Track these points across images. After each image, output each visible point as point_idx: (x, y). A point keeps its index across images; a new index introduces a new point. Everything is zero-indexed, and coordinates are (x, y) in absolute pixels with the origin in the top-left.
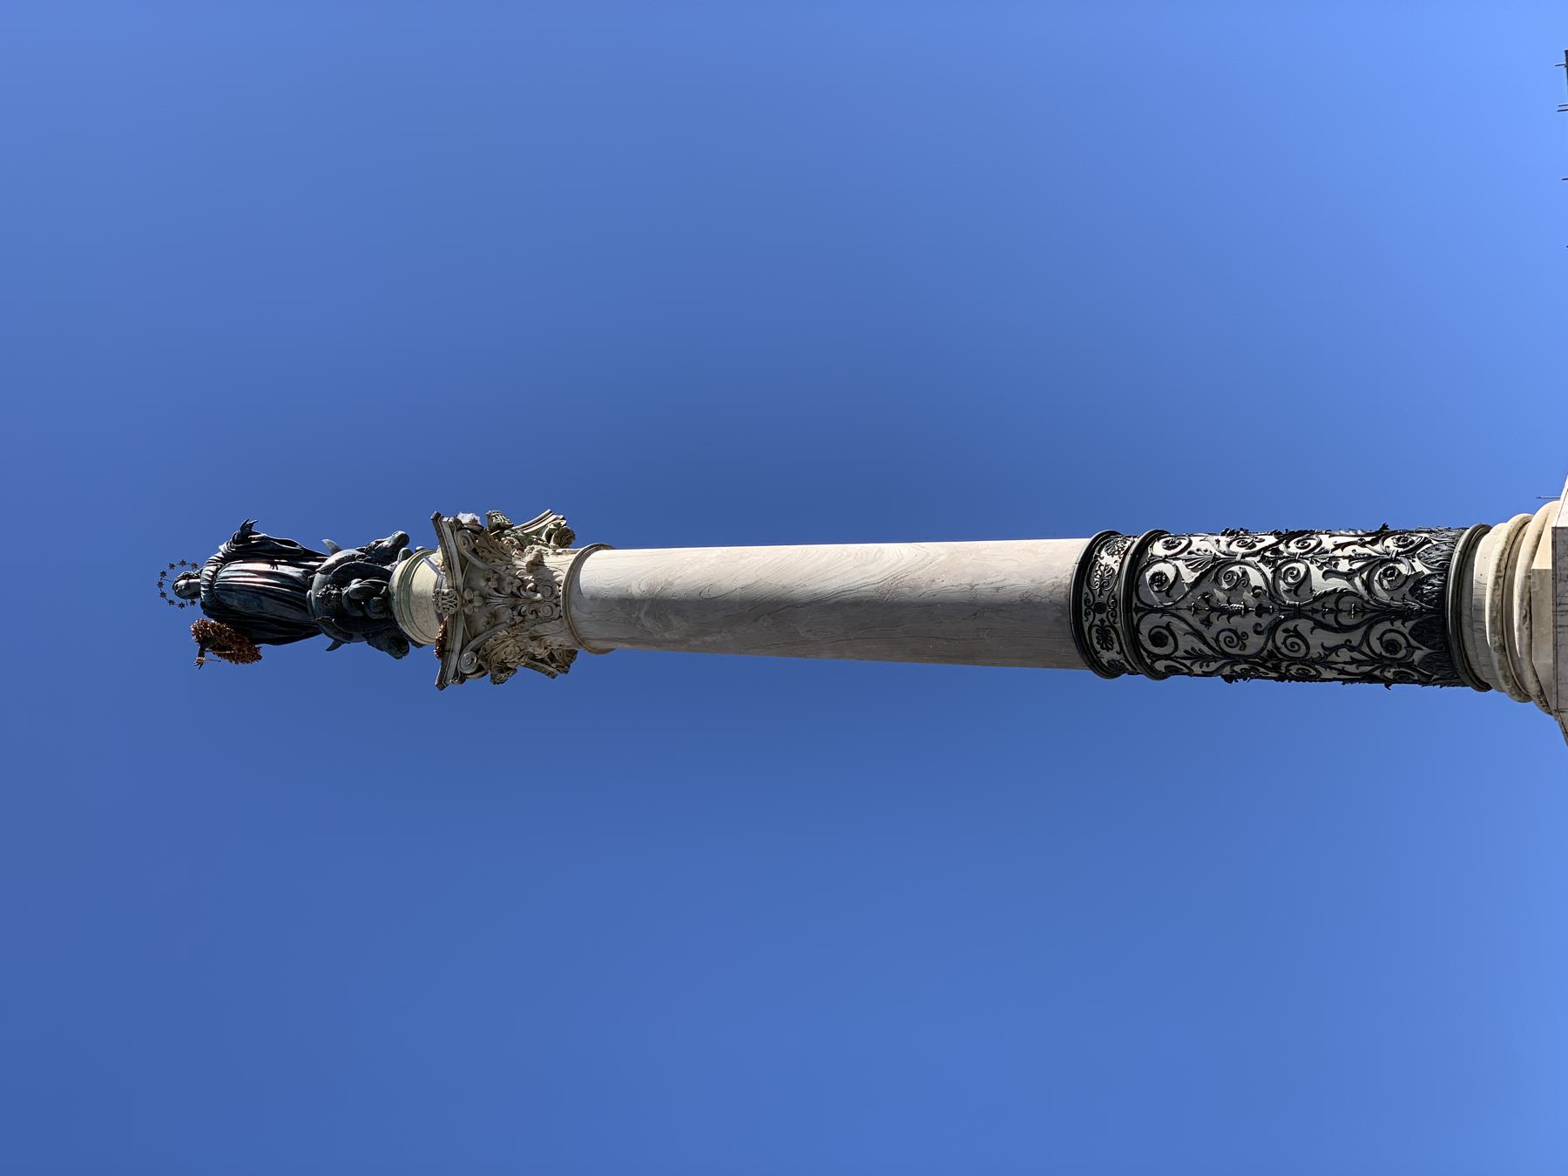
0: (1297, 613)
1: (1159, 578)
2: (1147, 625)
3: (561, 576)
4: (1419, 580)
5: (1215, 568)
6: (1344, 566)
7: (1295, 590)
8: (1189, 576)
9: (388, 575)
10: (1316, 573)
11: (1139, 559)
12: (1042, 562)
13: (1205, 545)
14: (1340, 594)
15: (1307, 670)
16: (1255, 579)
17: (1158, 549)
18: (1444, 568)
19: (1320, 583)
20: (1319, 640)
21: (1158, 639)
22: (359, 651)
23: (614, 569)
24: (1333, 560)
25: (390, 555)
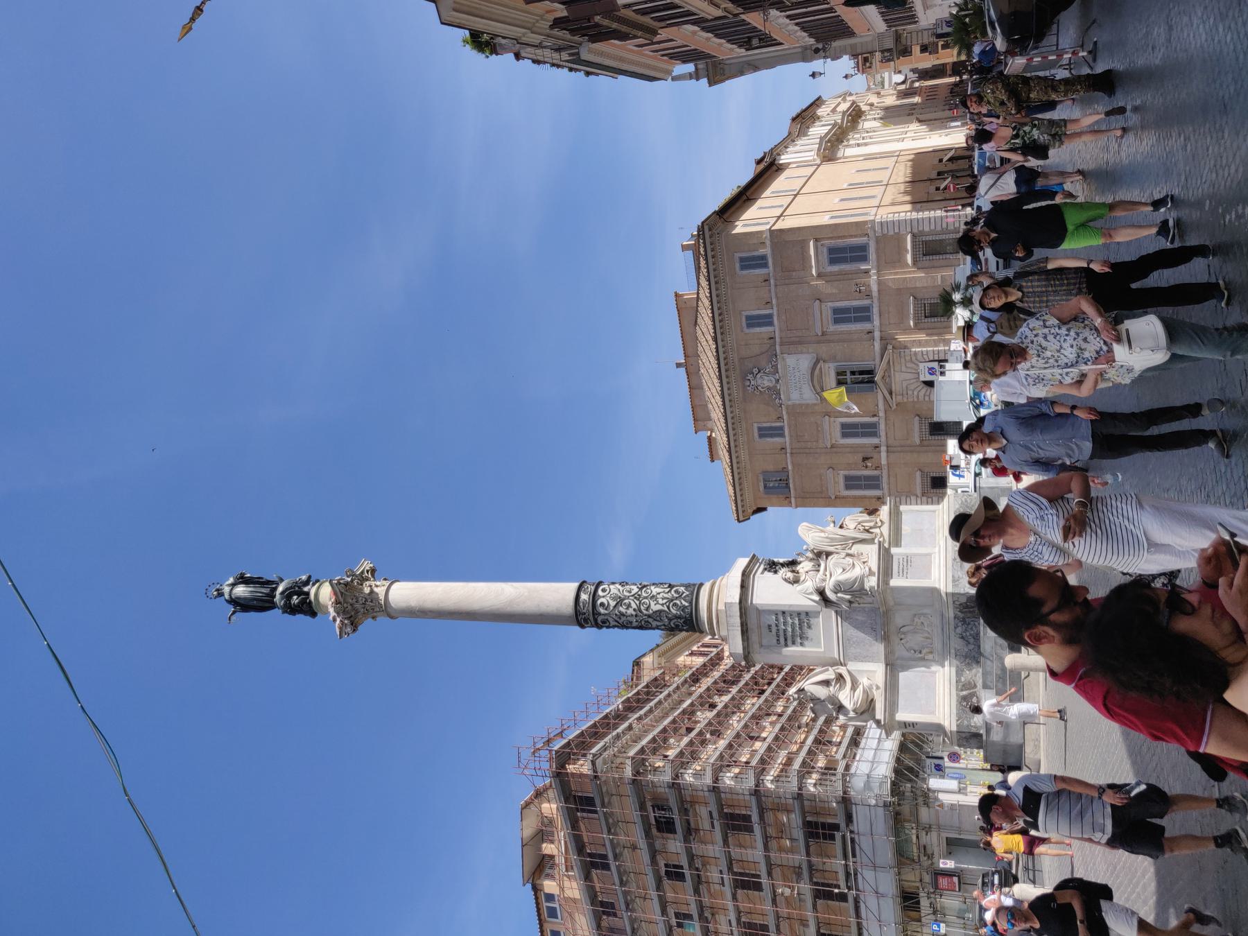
0: (649, 616)
1: (602, 604)
2: (600, 619)
3: (382, 597)
4: (685, 607)
5: (620, 601)
6: (661, 601)
7: (647, 609)
8: (613, 603)
9: (308, 594)
10: (652, 604)
11: (595, 596)
12: (558, 594)
13: (615, 589)
14: (660, 611)
16: (634, 606)
17: (600, 593)
18: (691, 603)
19: (655, 607)
20: (654, 624)
21: (604, 622)
22: (300, 617)
23: (403, 593)
24: (658, 599)
25: (307, 583)
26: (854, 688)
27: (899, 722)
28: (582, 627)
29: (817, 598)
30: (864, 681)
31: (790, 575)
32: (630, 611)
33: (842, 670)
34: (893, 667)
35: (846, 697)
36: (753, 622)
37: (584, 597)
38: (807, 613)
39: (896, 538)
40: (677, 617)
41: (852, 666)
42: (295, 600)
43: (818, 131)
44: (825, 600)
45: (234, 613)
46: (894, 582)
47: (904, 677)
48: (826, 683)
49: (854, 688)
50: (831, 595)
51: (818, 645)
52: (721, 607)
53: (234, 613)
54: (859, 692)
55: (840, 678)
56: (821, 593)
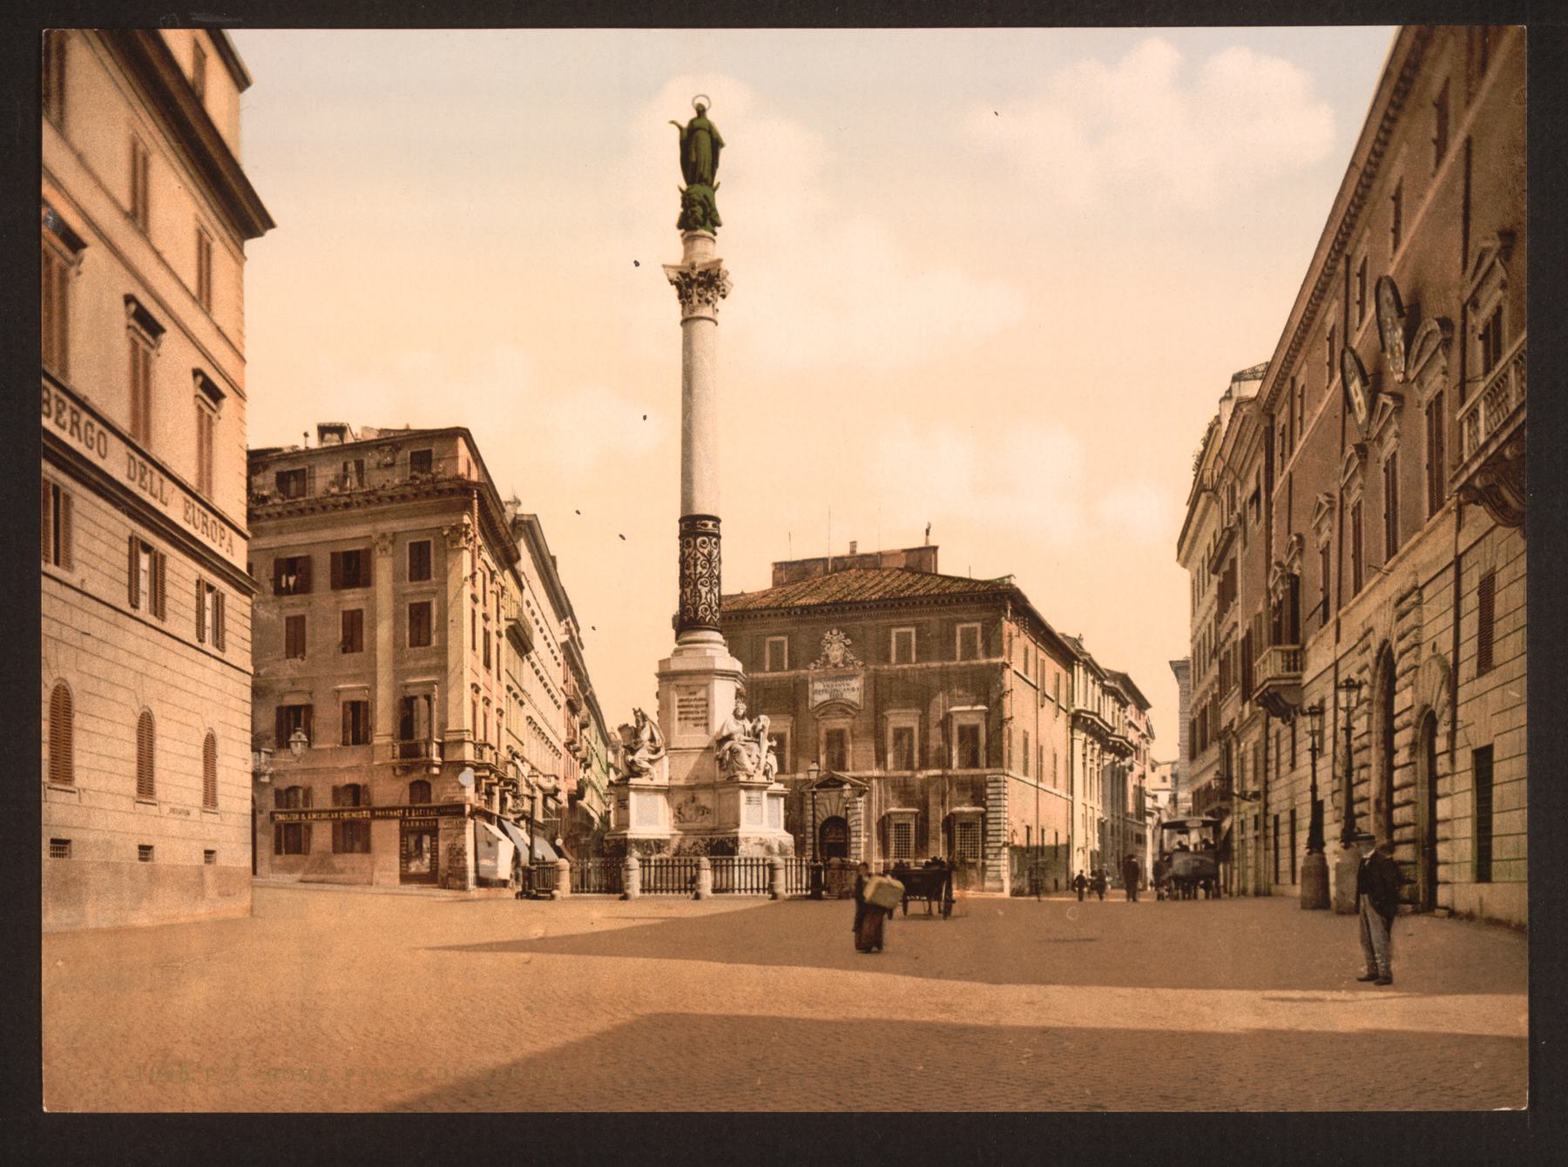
15: (682, 586)
19: (704, 590)
26: (651, 761)
27: (627, 798)
28: (681, 521)
29: (725, 733)
30: (654, 769)
31: (741, 712)
32: (699, 569)
33: (662, 752)
34: (668, 791)
35: (642, 756)
36: (702, 680)
37: (710, 524)
38: (707, 725)
39: (771, 796)
40: (696, 611)
41: (666, 759)
42: (699, 210)
43: (1109, 711)
44: (722, 741)
45: (680, 128)
46: (743, 794)
47: (661, 799)
48: (652, 739)
49: (651, 761)
50: (727, 745)
51: (681, 731)
52: (709, 653)
53: (680, 128)
54: (645, 765)
55: (657, 751)
56: (729, 738)
